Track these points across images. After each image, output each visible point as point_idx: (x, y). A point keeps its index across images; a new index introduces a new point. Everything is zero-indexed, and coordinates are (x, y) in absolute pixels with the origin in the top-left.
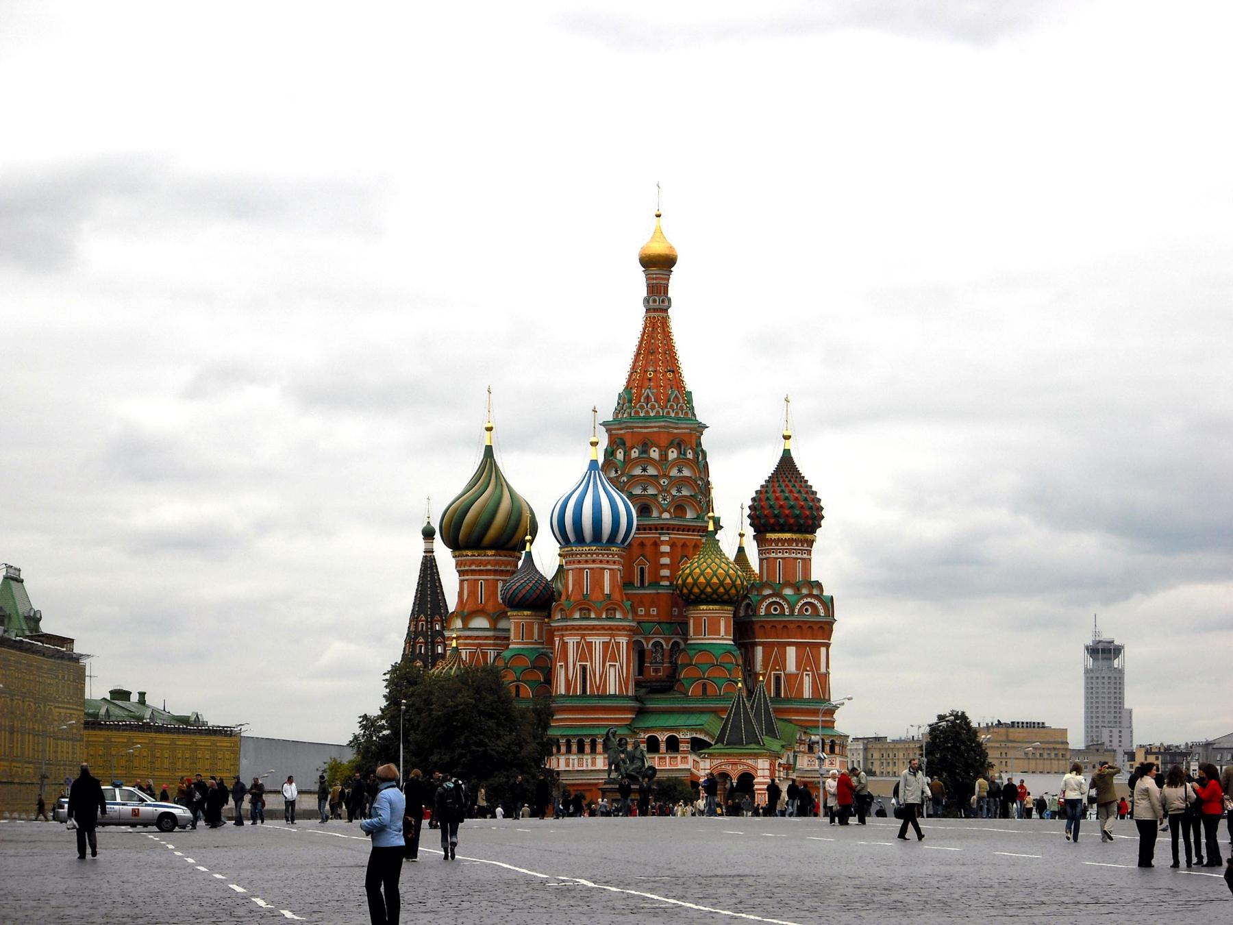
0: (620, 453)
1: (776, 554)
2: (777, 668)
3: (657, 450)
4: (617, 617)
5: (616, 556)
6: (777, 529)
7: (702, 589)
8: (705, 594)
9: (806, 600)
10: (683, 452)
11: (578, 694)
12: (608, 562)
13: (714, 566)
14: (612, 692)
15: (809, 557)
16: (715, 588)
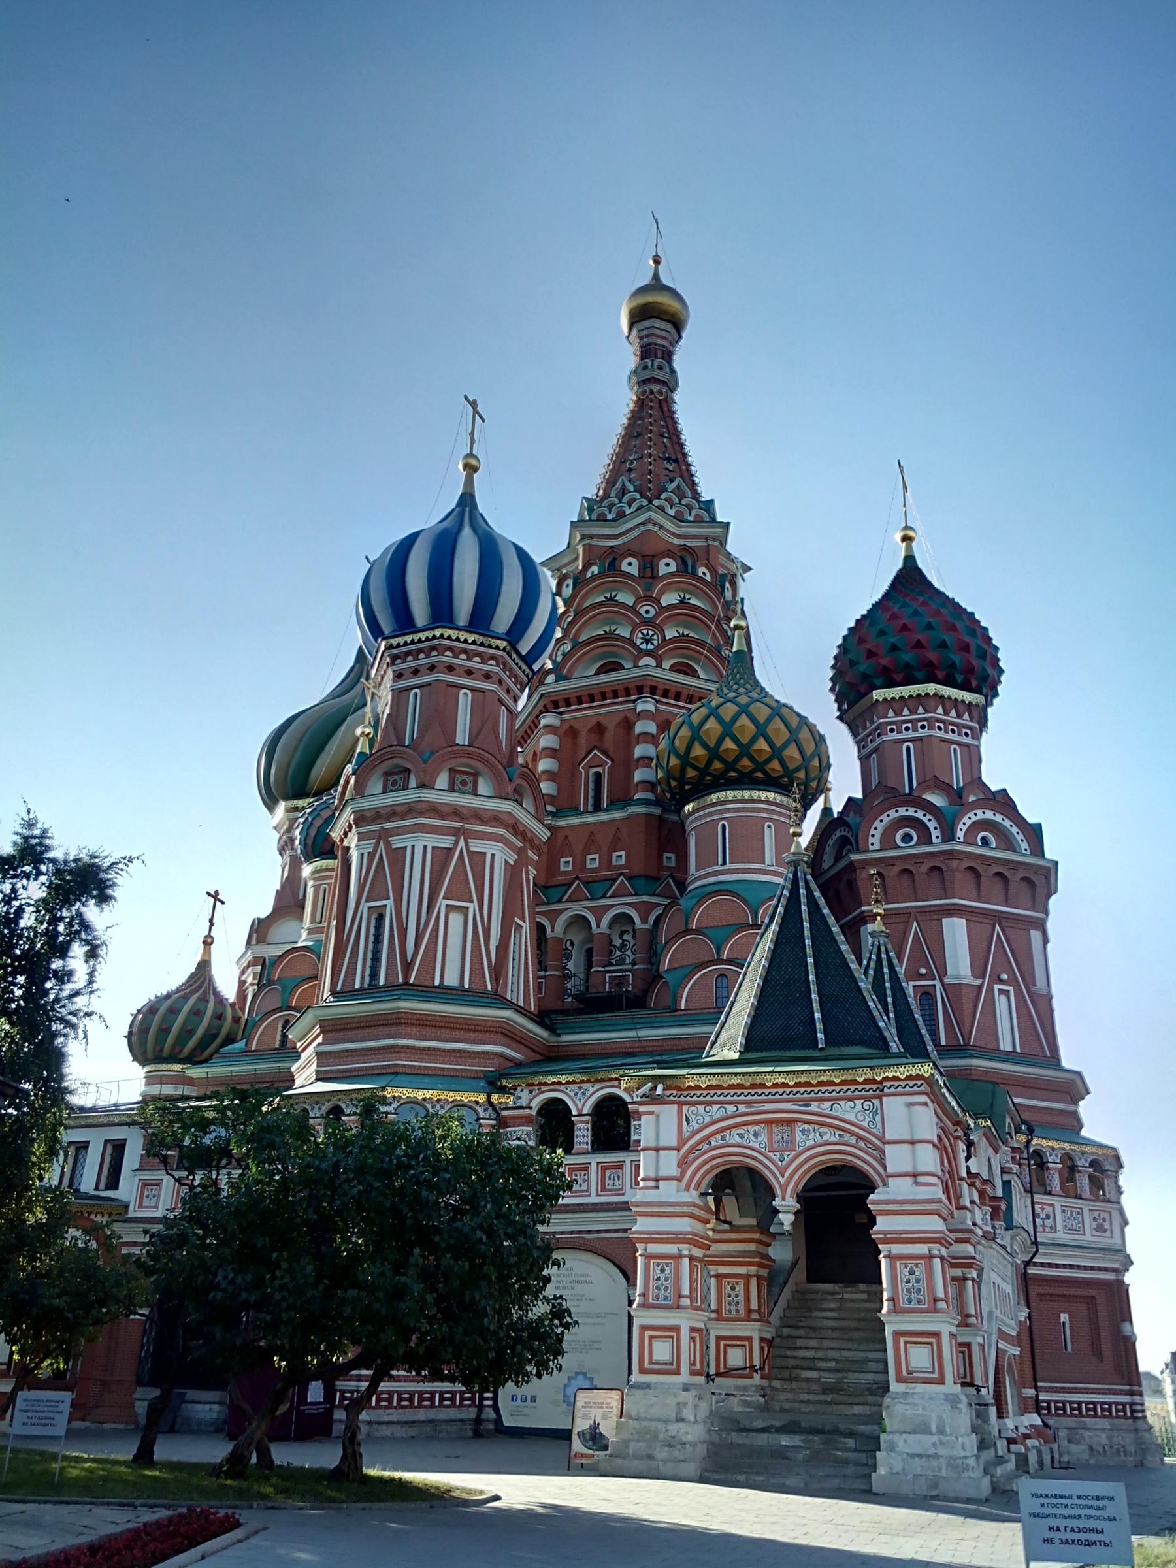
0: (568, 586)
1: (900, 732)
2: (923, 971)
3: (634, 561)
4: (484, 787)
5: (492, 662)
6: (898, 677)
7: (712, 746)
8: (722, 761)
9: (981, 815)
10: (690, 570)
11: (357, 986)
12: (469, 672)
13: (744, 700)
14: (451, 980)
15: (975, 742)
16: (745, 741)
